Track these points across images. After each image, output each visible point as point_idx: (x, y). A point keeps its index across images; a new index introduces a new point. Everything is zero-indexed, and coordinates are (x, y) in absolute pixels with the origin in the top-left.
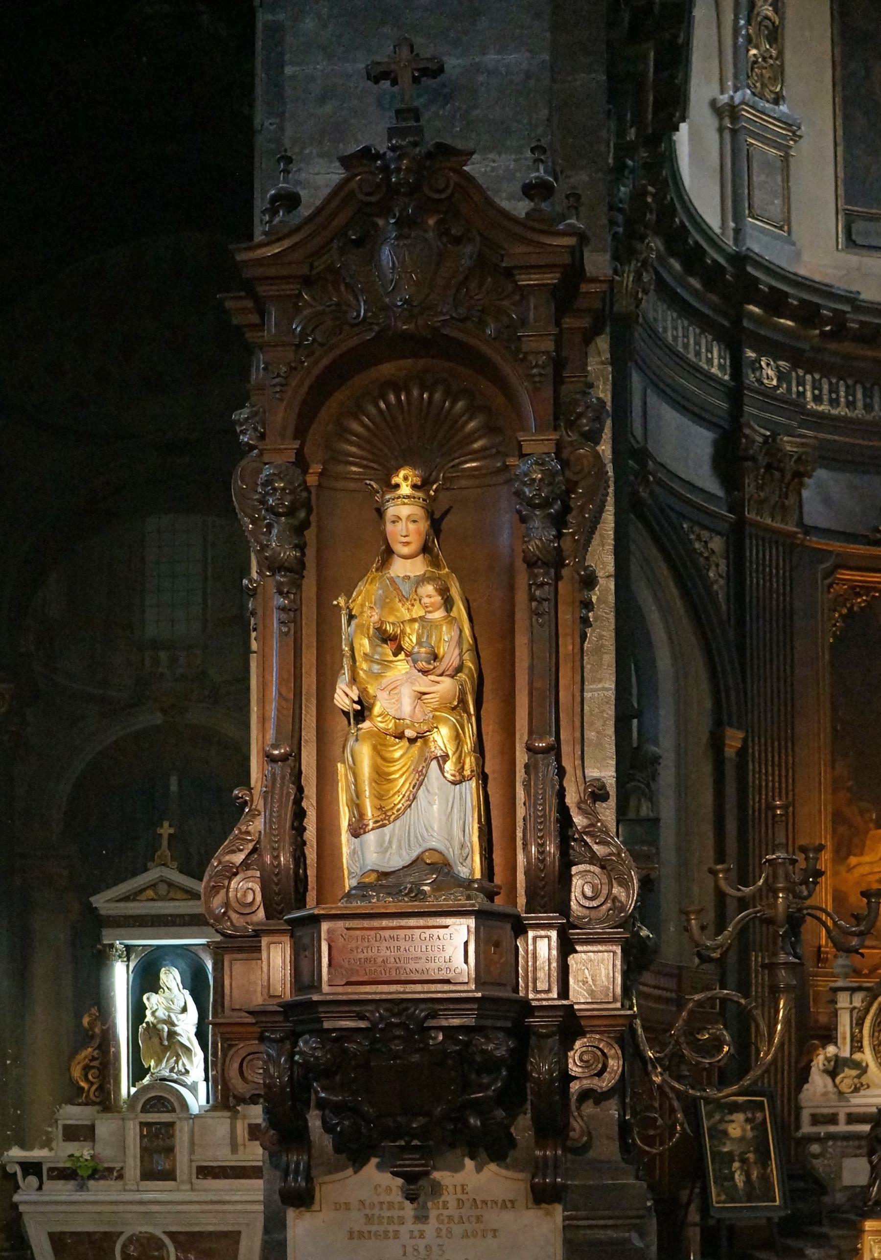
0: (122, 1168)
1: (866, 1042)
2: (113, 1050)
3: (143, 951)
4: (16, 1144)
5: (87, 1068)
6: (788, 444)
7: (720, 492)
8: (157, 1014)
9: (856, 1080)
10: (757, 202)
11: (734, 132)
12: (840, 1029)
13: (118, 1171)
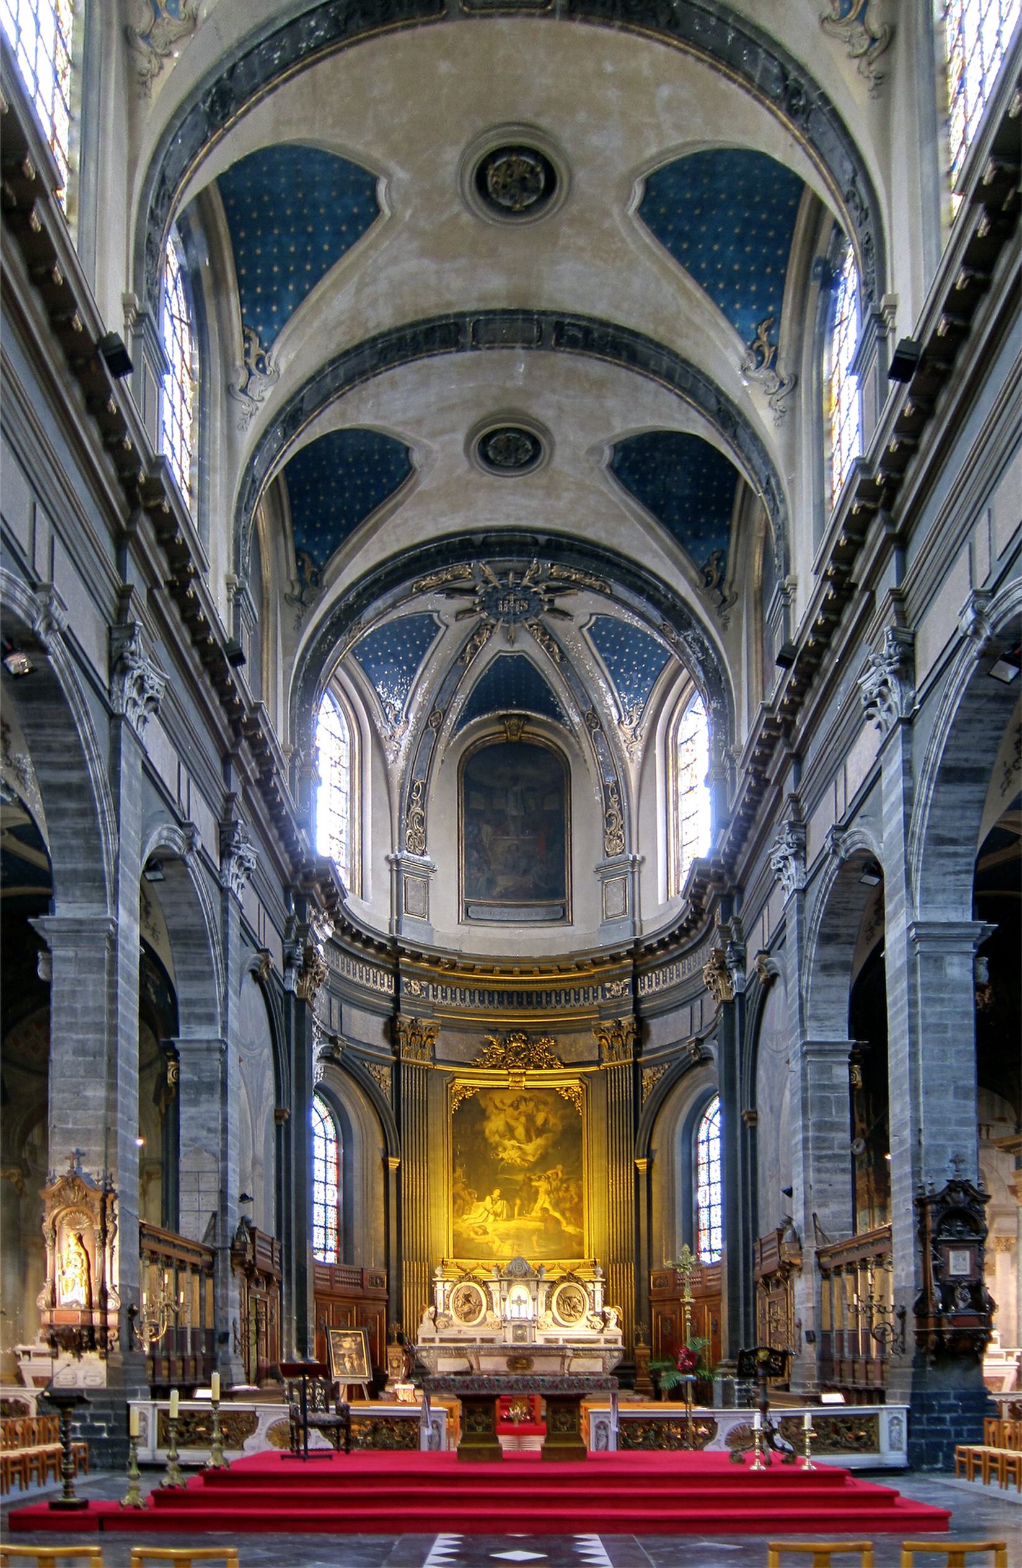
6: (425, 1022)
7: (388, 1047)
10: (409, 906)
11: (398, 872)
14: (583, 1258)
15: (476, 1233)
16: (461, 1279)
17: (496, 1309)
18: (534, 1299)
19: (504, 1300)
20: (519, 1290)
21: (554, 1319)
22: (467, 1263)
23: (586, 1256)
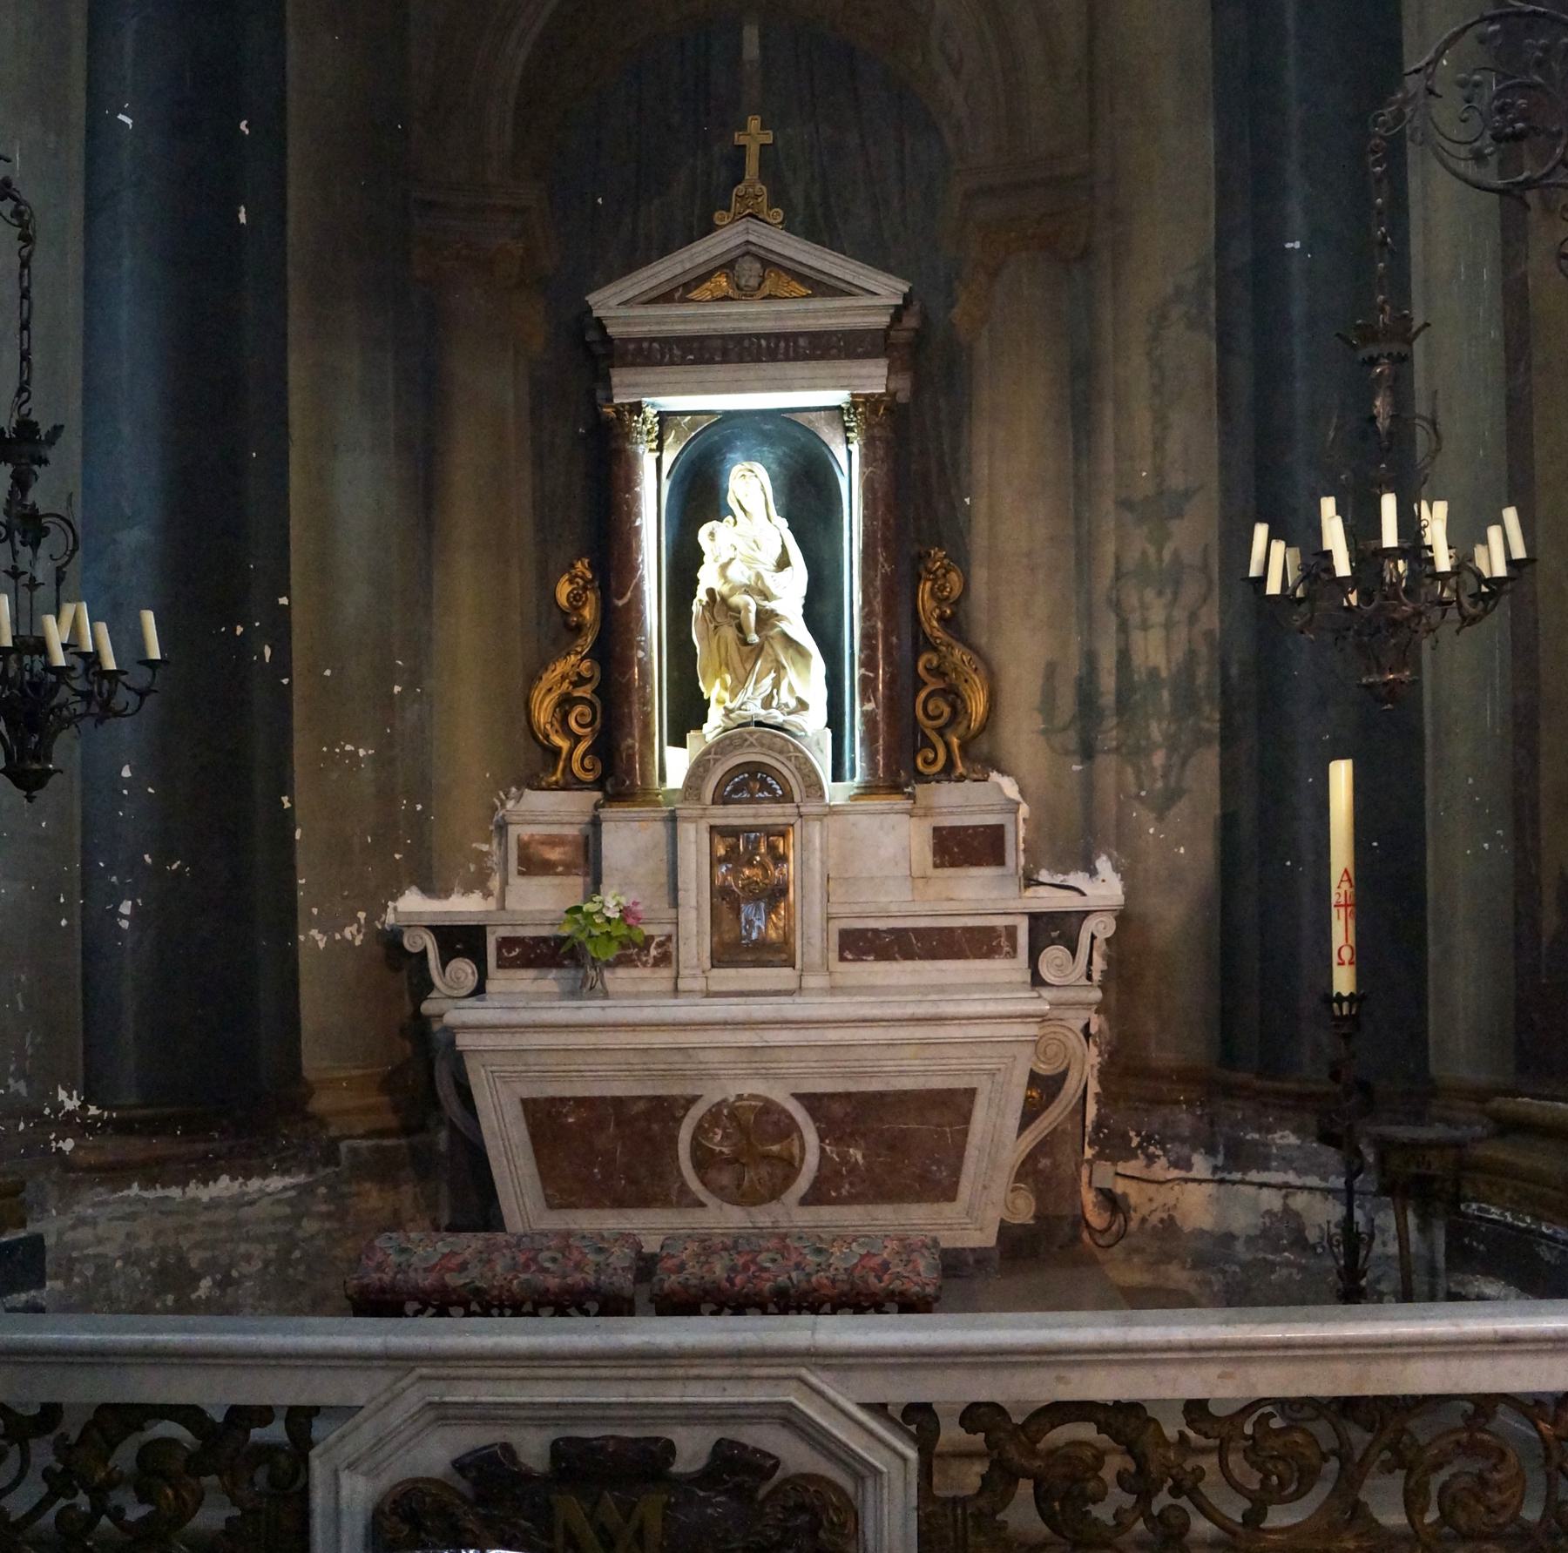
0: (669, 938)
2: (641, 654)
3: (692, 427)
4: (413, 883)
5: (565, 704)
8: (730, 572)
13: (660, 945)
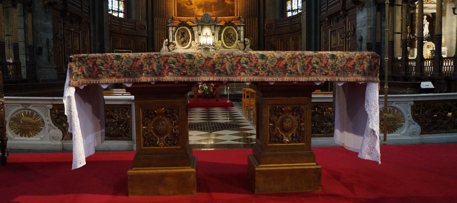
1: (175, 39)
9: (173, 47)
12: (170, 36)
14: (234, 16)
15: (187, 4)
16: (180, 25)
17: (196, 40)
18: (213, 35)
19: (200, 35)
20: (207, 31)
21: (222, 44)
22: (184, 18)
23: (236, 15)
